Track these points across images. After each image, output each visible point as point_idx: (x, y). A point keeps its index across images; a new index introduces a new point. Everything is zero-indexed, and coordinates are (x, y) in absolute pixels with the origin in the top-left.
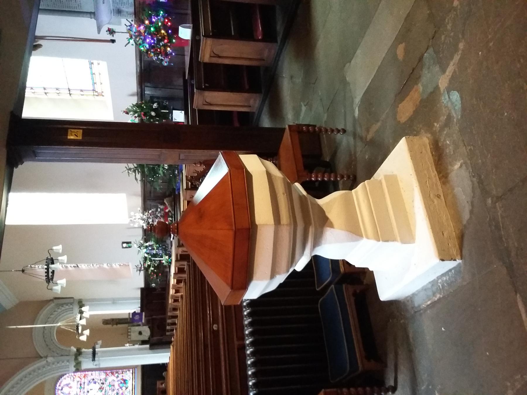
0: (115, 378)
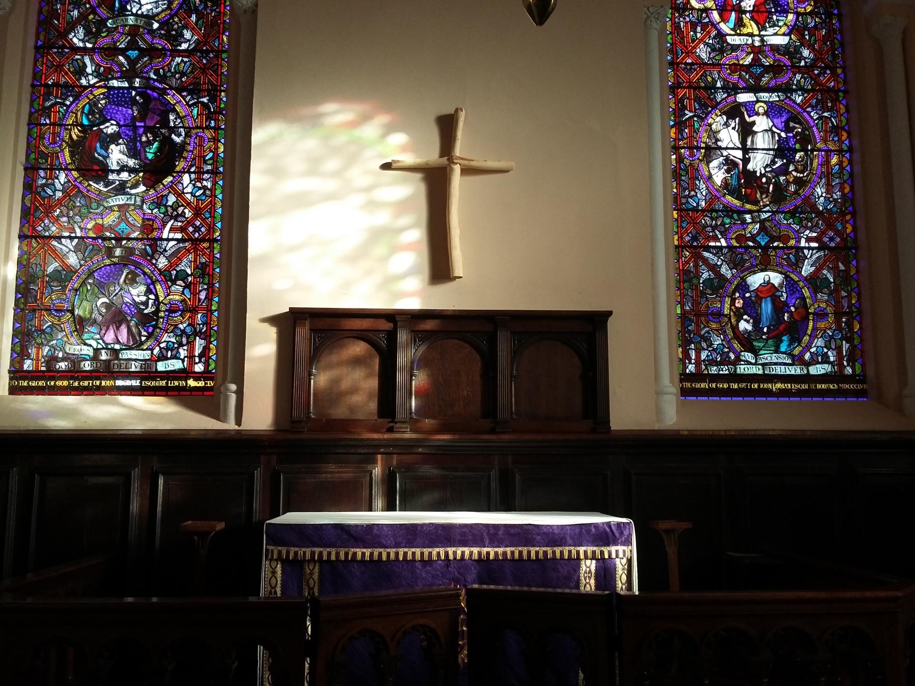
0: (807, 269)
